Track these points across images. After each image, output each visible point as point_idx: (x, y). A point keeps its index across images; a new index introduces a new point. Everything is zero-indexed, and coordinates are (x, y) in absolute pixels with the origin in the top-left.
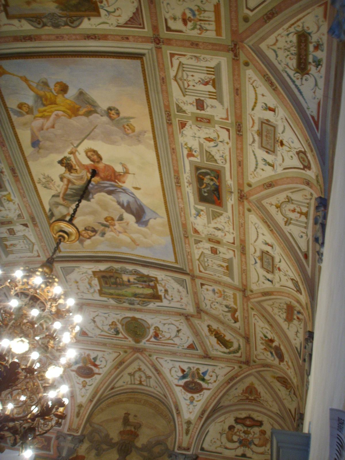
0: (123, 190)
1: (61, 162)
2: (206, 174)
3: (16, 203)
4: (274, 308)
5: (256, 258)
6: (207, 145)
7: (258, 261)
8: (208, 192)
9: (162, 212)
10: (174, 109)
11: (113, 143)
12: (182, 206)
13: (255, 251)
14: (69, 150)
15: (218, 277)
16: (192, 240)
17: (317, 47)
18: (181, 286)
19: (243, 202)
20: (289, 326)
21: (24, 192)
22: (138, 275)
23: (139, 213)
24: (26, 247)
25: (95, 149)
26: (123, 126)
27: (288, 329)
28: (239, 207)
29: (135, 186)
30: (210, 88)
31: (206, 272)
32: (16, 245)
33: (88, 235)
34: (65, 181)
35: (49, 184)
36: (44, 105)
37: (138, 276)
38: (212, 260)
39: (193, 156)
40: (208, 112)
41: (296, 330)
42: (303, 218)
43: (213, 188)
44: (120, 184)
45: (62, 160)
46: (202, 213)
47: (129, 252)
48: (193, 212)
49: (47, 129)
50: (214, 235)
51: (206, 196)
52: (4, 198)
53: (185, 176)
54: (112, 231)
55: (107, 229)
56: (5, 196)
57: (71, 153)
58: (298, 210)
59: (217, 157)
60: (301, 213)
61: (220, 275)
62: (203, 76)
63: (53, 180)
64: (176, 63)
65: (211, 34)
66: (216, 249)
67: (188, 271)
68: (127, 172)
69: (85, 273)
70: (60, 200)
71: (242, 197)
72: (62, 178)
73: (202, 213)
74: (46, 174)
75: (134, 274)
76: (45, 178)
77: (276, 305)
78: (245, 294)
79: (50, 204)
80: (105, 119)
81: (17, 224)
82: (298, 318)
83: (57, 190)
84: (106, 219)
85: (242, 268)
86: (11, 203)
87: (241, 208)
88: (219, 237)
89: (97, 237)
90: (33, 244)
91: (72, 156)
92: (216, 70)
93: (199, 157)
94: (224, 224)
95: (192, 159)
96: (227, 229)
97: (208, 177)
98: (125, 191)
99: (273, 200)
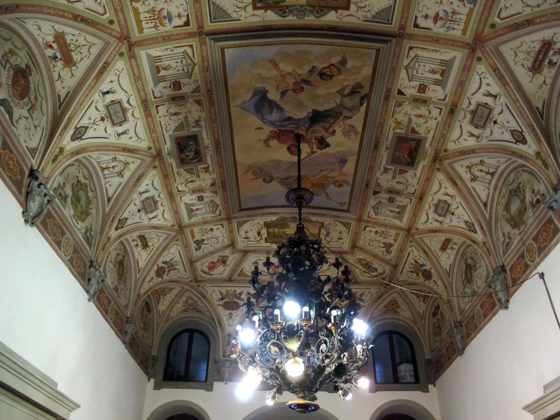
0: (273, 124)
1: (328, 145)
2: (192, 159)
3: (394, 118)
4: (86, 43)
5: (131, 107)
6: (194, 178)
7: (126, 105)
8: (189, 145)
9: (234, 111)
10: (220, 191)
11: (273, 161)
12: (214, 125)
13: (133, 115)
14: (315, 155)
15: (167, 49)
16: (203, 90)
17: (137, 245)
18: (218, 6)
19: (157, 152)
20: (55, 30)
21: (378, 127)
22: (283, 7)
23: (262, 103)
24: (419, 65)
25: (291, 155)
26: (261, 172)
27: (53, 27)
28: (160, 146)
29: (261, 131)
30: (194, 208)
31: (182, 50)
32: (430, 70)
33: (331, 70)
34: (331, 130)
35: (349, 130)
36: (322, 184)
37: (282, 4)
38: (178, 72)
39: (204, 168)
40: (195, 196)
41: (42, 29)
42: (104, 166)
43: (186, 150)
44: (275, 129)
45: (325, 148)
46: (194, 124)
47: (286, 46)
48: (202, 123)
49: (327, 170)
50: (179, 106)
51: (191, 141)
52: (402, 127)
53: (211, 152)
54: (299, 75)
55: (305, 78)
56: (400, 128)
57: (313, 152)
58: (111, 169)
59: (185, 173)
60: (107, 168)
61: (165, 53)
62: (199, 212)
63: (343, 132)
64: (218, 213)
65: (196, 229)
66: (175, 90)
67: (207, 39)
68: (266, 142)
69: (361, 8)
70: (345, 113)
71: (159, 155)
72: (334, 132)
73: (194, 124)
74: (346, 138)
75: (287, 7)
76: (350, 135)
77: (85, 50)
78: (128, 42)
79: (359, 110)
80: (275, 176)
81: (409, 96)
82: (51, 47)
83: (344, 123)
84: (302, 89)
85: (142, 81)
86: (399, 120)
87: (158, 146)
88: (173, 106)
89: (320, 66)
90: (406, 68)
91: (315, 150)
92: (190, 217)
93: (199, 168)
94: (171, 122)
95: (205, 166)
96: (167, 118)
97: (190, 157)
98: (272, 123)
99: (132, 167)
